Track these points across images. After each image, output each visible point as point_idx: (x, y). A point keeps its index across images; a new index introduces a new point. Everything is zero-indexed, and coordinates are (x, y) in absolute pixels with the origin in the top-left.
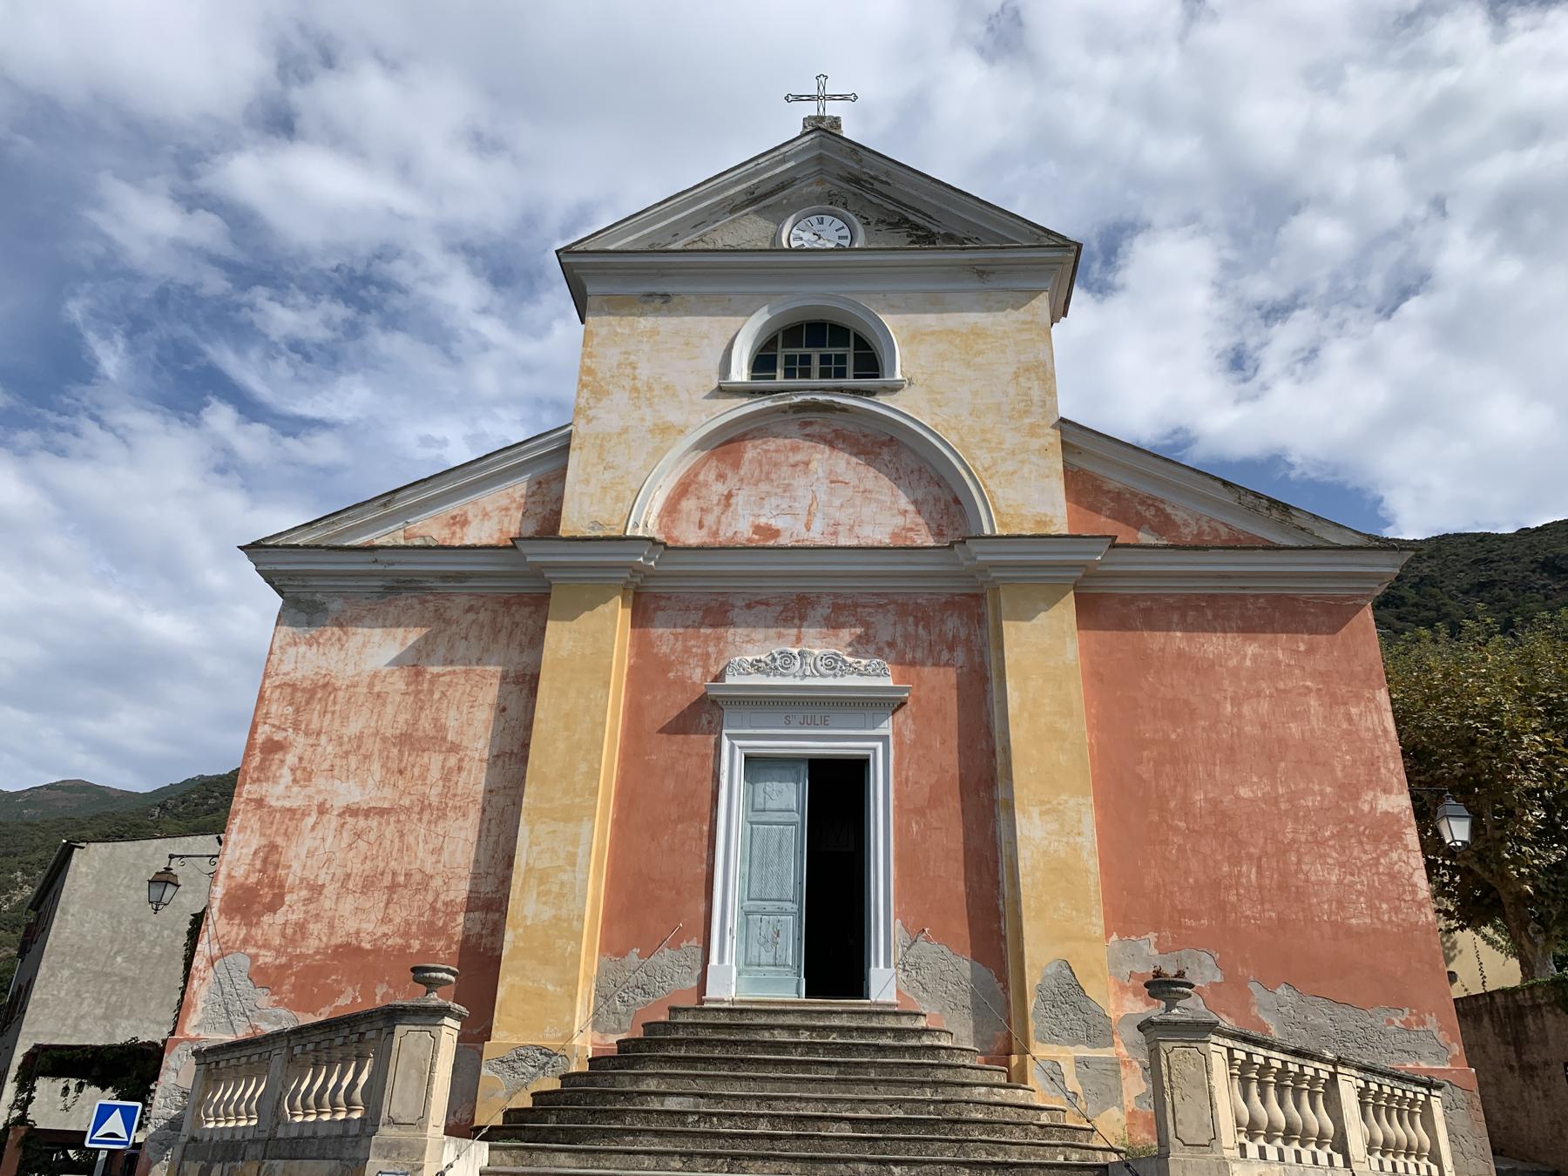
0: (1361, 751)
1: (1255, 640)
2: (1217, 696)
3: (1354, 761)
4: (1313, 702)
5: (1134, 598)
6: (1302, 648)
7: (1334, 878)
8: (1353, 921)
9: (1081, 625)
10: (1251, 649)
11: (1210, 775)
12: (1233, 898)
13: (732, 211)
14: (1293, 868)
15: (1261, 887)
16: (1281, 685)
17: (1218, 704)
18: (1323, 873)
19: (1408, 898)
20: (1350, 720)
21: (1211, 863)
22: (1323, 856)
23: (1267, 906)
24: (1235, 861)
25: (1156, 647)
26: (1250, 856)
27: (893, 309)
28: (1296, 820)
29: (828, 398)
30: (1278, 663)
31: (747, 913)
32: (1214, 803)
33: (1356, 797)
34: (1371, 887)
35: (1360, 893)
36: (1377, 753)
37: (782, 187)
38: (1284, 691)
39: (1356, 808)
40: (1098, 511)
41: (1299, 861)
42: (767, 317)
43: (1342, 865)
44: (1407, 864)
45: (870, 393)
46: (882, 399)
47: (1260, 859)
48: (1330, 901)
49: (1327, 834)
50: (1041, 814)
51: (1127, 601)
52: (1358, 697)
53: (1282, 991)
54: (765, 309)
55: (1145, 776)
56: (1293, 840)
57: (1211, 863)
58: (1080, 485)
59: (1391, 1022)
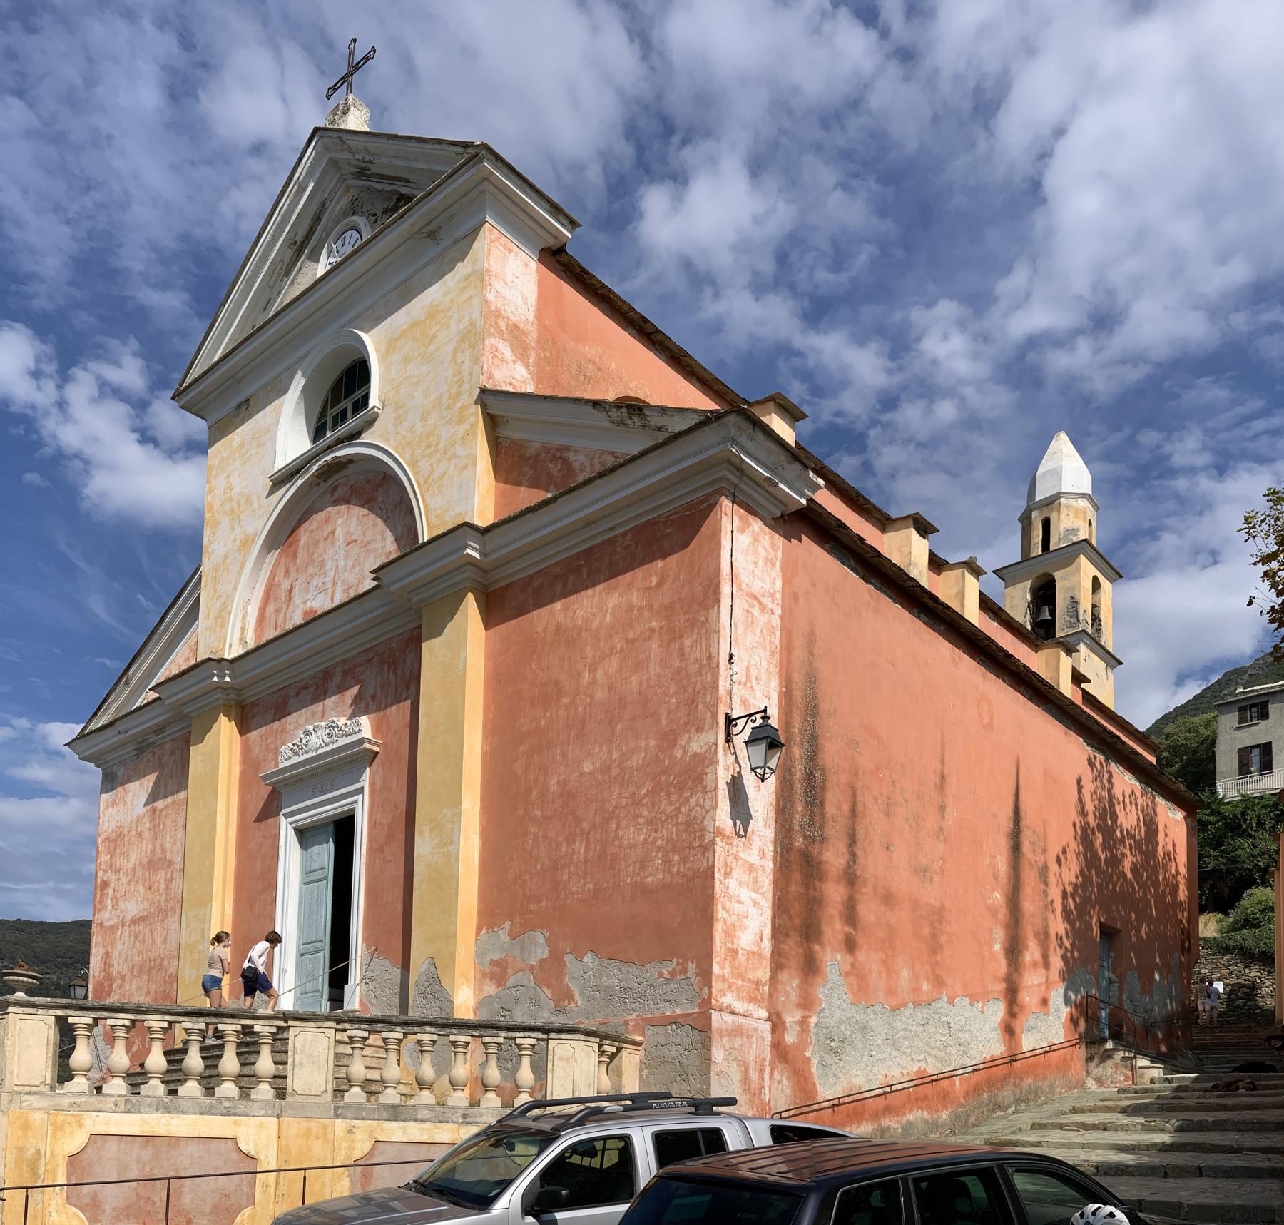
0: (685, 688)
1: (615, 588)
2: (579, 667)
3: (678, 703)
4: (654, 645)
5: (531, 578)
6: (654, 581)
7: (642, 838)
8: (650, 879)
9: (487, 626)
10: (613, 600)
11: (564, 756)
12: (565, 877)
13: (287, 274)
14: (612, 835)
15: (586, 861)
16: (631, 635)
17: (579, 675)
18: (633, 835)
19: (696, 844)
20: (682, 654)
21: (554, 846)
22: (636, 817)
23: (589, 879)
24: (571, 839)
25: (540, 629)
26: (582, 831)
27: (367, 331)
28: (622, 784)
29: (333, 455)
30: (630, 608)
31: (302, 955)
32: (563, 784)
33: (673, 744)
34: (669, 840)
35: (659, 849)
36: (699, 687)
37: (317, 218)
38: (634, 641)
39: (671, 756)
40: (519, 484)
41: (617, 828)
42: (303, 381)
43: (649, 822)
44: (702, 806)
45: (353, 436)
46: (365, 438)
47: (589, 833)
48: (635, 863)
49: (644, 792)
50: (431, 830)
51: (525, 584)
52: (693, 623)
53: (588, 958)
54: (299, 374)
55: (519, 772)
56: (616, 807)
57: (554, 846)
58: (509, 460)
59: (661, 974)
